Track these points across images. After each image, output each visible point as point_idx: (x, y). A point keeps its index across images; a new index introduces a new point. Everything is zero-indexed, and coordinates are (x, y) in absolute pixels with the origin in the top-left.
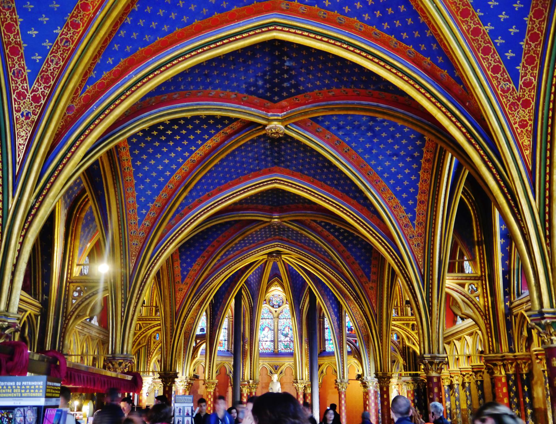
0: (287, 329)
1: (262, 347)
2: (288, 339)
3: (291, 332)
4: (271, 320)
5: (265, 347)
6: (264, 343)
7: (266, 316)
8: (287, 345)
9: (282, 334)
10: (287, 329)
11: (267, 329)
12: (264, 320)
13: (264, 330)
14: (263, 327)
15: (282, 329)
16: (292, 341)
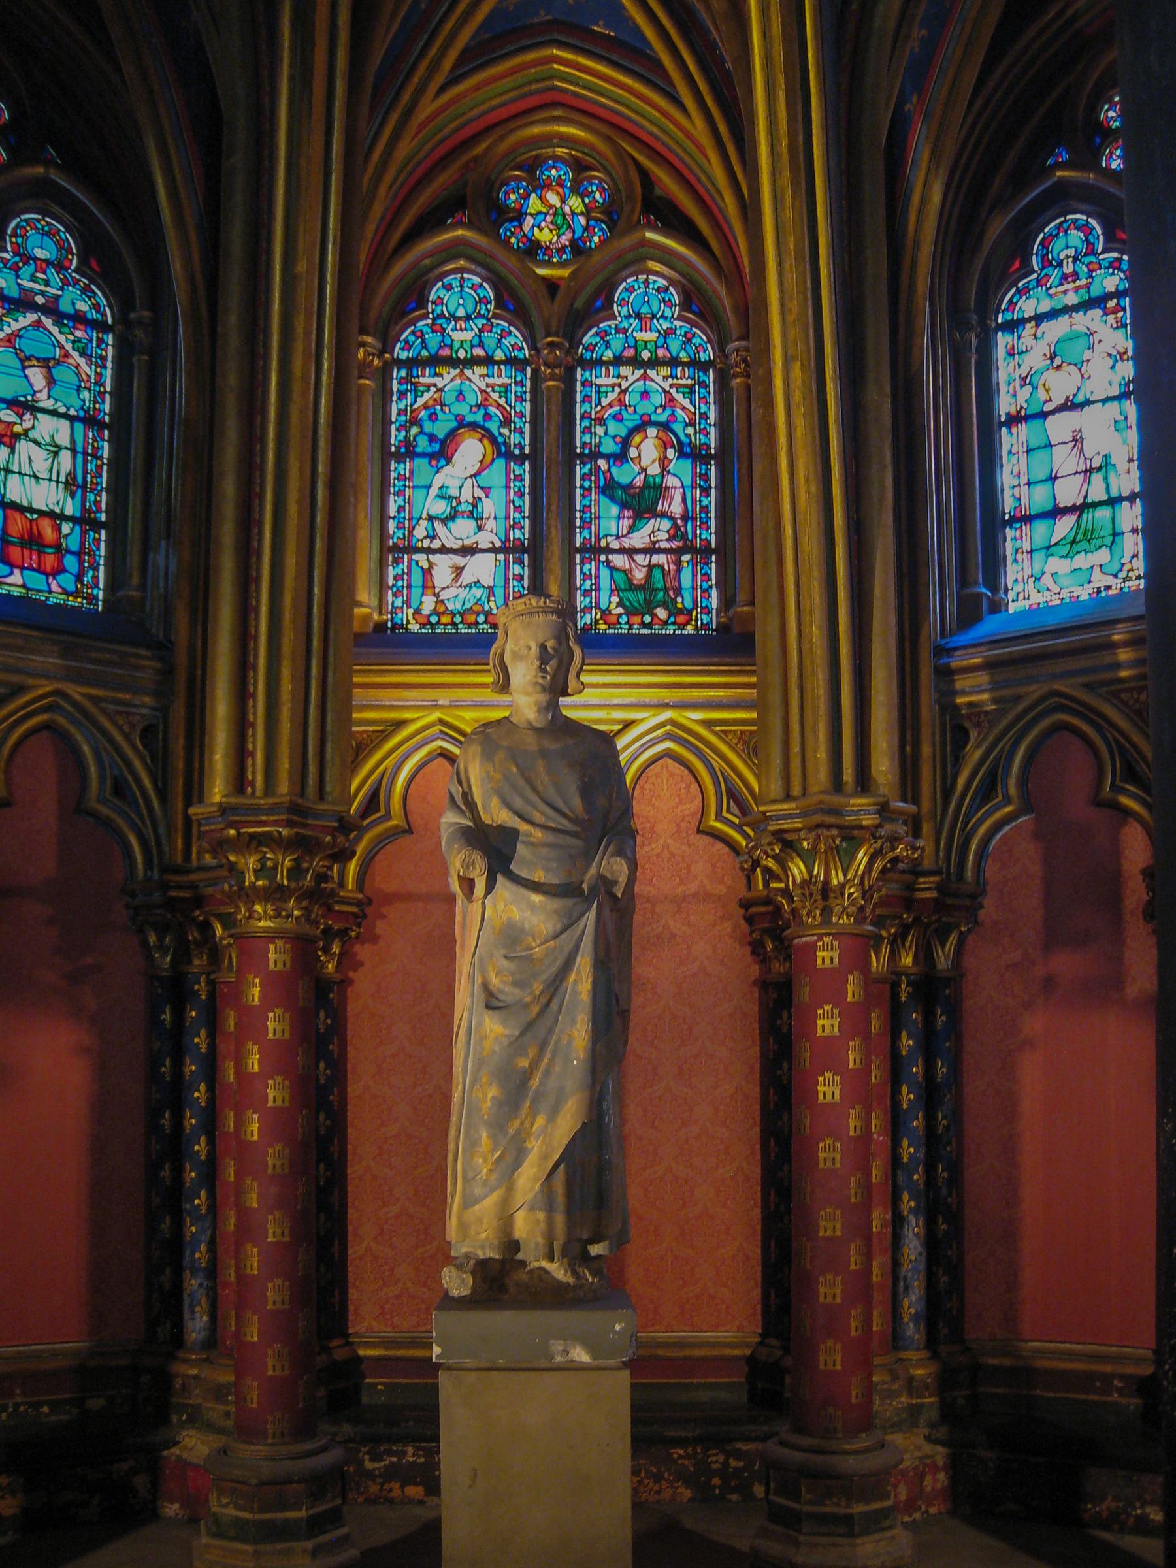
0: (648, 450)
1: (428, 604)
2: (655, 530)
3: (682, 469)
4: (504, 376)
5: (456, 599)
6: (443, 567)
7: (461, 336)
8: (646, 587)
9: (609, 488)
10: (648, 450)
11: (471, 450)
12: (447, 378)
13: (444, 452)
14: (441, 429)
15: (609, 447)
16: (703, 553)
